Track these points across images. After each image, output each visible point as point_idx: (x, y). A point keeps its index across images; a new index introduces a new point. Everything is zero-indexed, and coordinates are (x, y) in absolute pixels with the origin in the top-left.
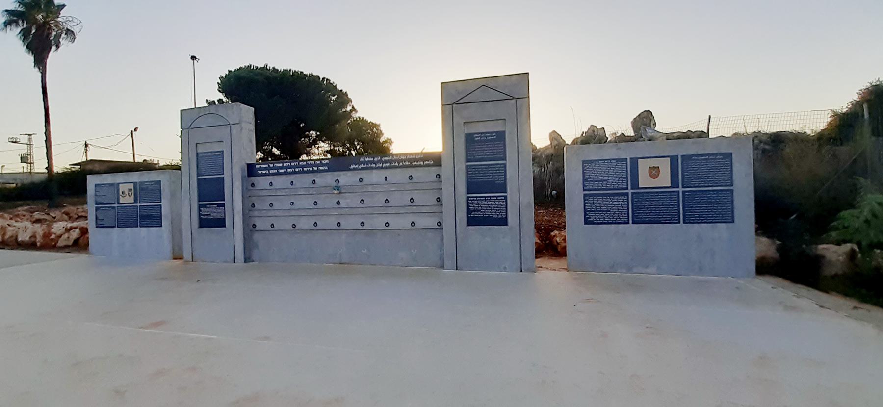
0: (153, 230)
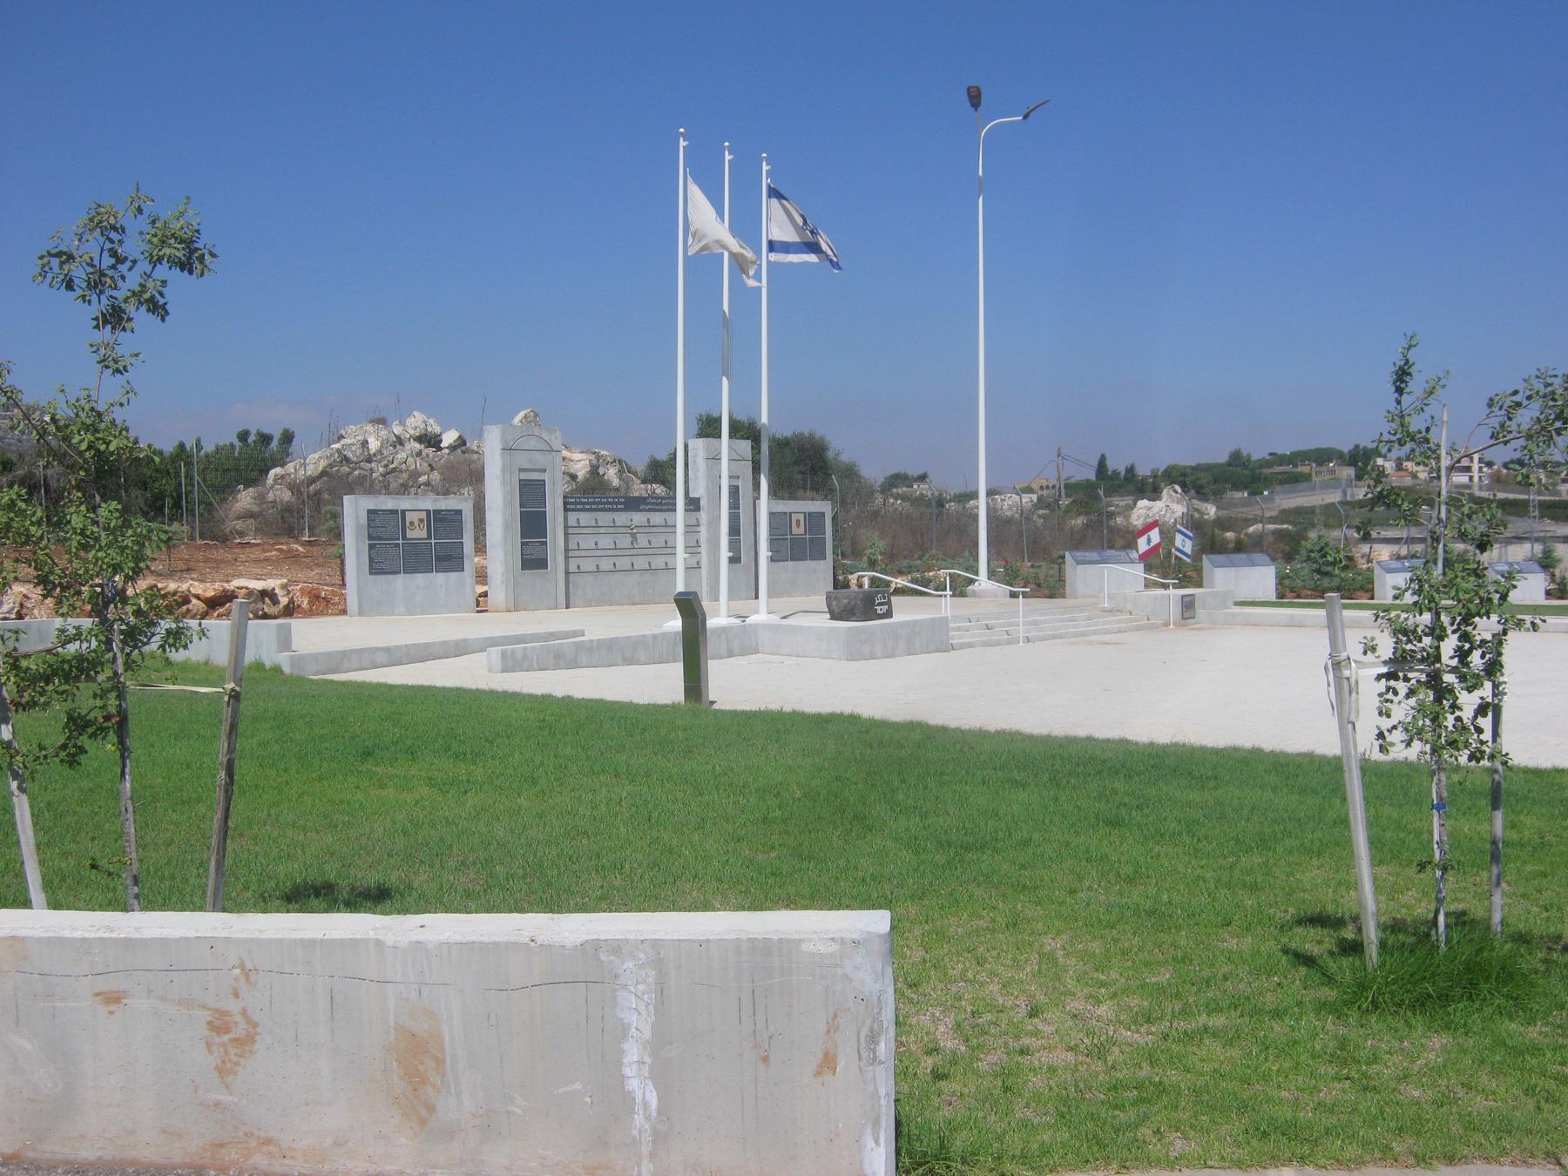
0: (453, 575)
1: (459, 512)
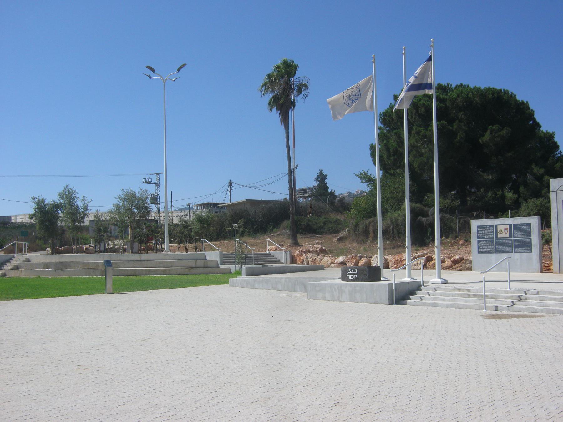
0: (525, 255)
1: (529, 224)
